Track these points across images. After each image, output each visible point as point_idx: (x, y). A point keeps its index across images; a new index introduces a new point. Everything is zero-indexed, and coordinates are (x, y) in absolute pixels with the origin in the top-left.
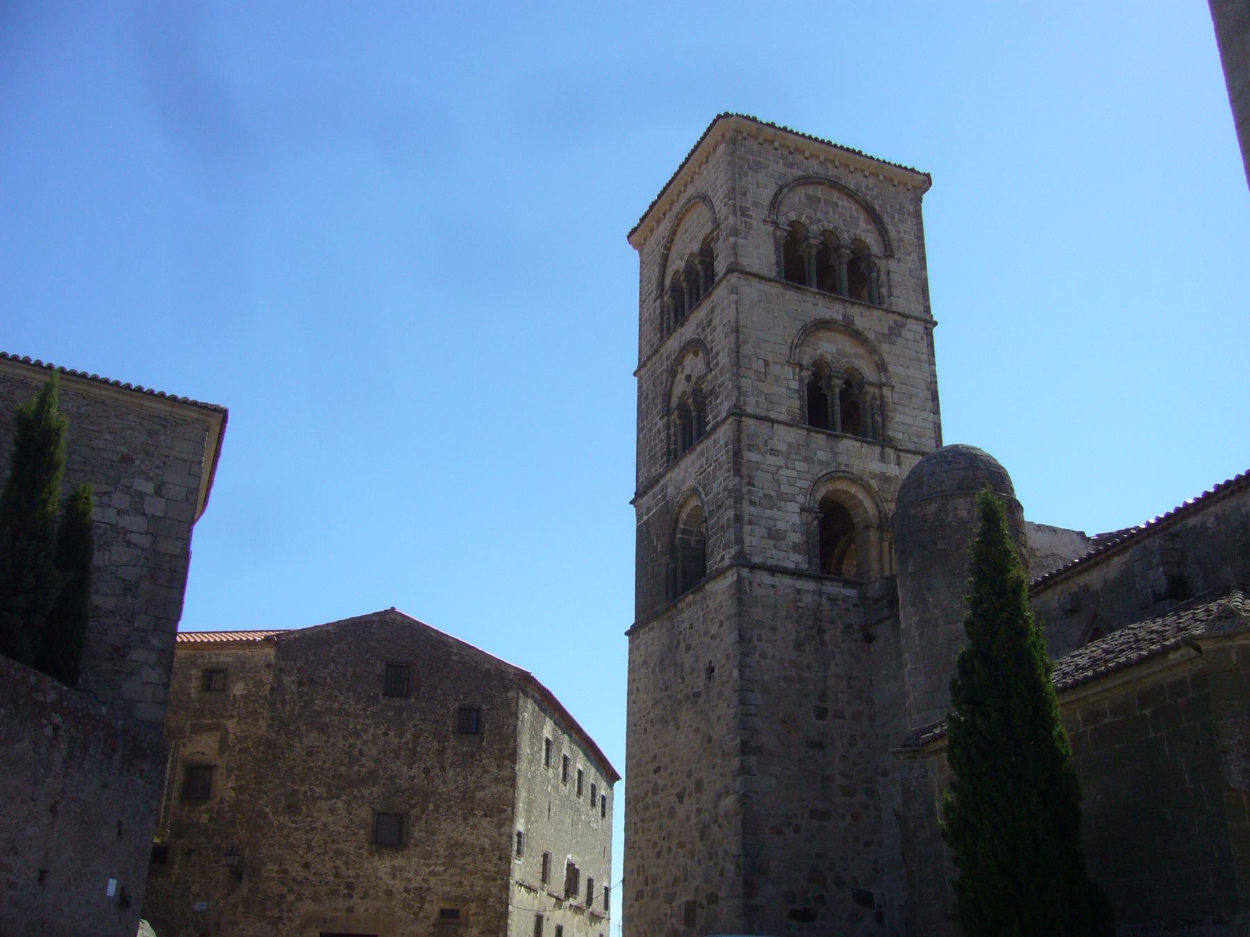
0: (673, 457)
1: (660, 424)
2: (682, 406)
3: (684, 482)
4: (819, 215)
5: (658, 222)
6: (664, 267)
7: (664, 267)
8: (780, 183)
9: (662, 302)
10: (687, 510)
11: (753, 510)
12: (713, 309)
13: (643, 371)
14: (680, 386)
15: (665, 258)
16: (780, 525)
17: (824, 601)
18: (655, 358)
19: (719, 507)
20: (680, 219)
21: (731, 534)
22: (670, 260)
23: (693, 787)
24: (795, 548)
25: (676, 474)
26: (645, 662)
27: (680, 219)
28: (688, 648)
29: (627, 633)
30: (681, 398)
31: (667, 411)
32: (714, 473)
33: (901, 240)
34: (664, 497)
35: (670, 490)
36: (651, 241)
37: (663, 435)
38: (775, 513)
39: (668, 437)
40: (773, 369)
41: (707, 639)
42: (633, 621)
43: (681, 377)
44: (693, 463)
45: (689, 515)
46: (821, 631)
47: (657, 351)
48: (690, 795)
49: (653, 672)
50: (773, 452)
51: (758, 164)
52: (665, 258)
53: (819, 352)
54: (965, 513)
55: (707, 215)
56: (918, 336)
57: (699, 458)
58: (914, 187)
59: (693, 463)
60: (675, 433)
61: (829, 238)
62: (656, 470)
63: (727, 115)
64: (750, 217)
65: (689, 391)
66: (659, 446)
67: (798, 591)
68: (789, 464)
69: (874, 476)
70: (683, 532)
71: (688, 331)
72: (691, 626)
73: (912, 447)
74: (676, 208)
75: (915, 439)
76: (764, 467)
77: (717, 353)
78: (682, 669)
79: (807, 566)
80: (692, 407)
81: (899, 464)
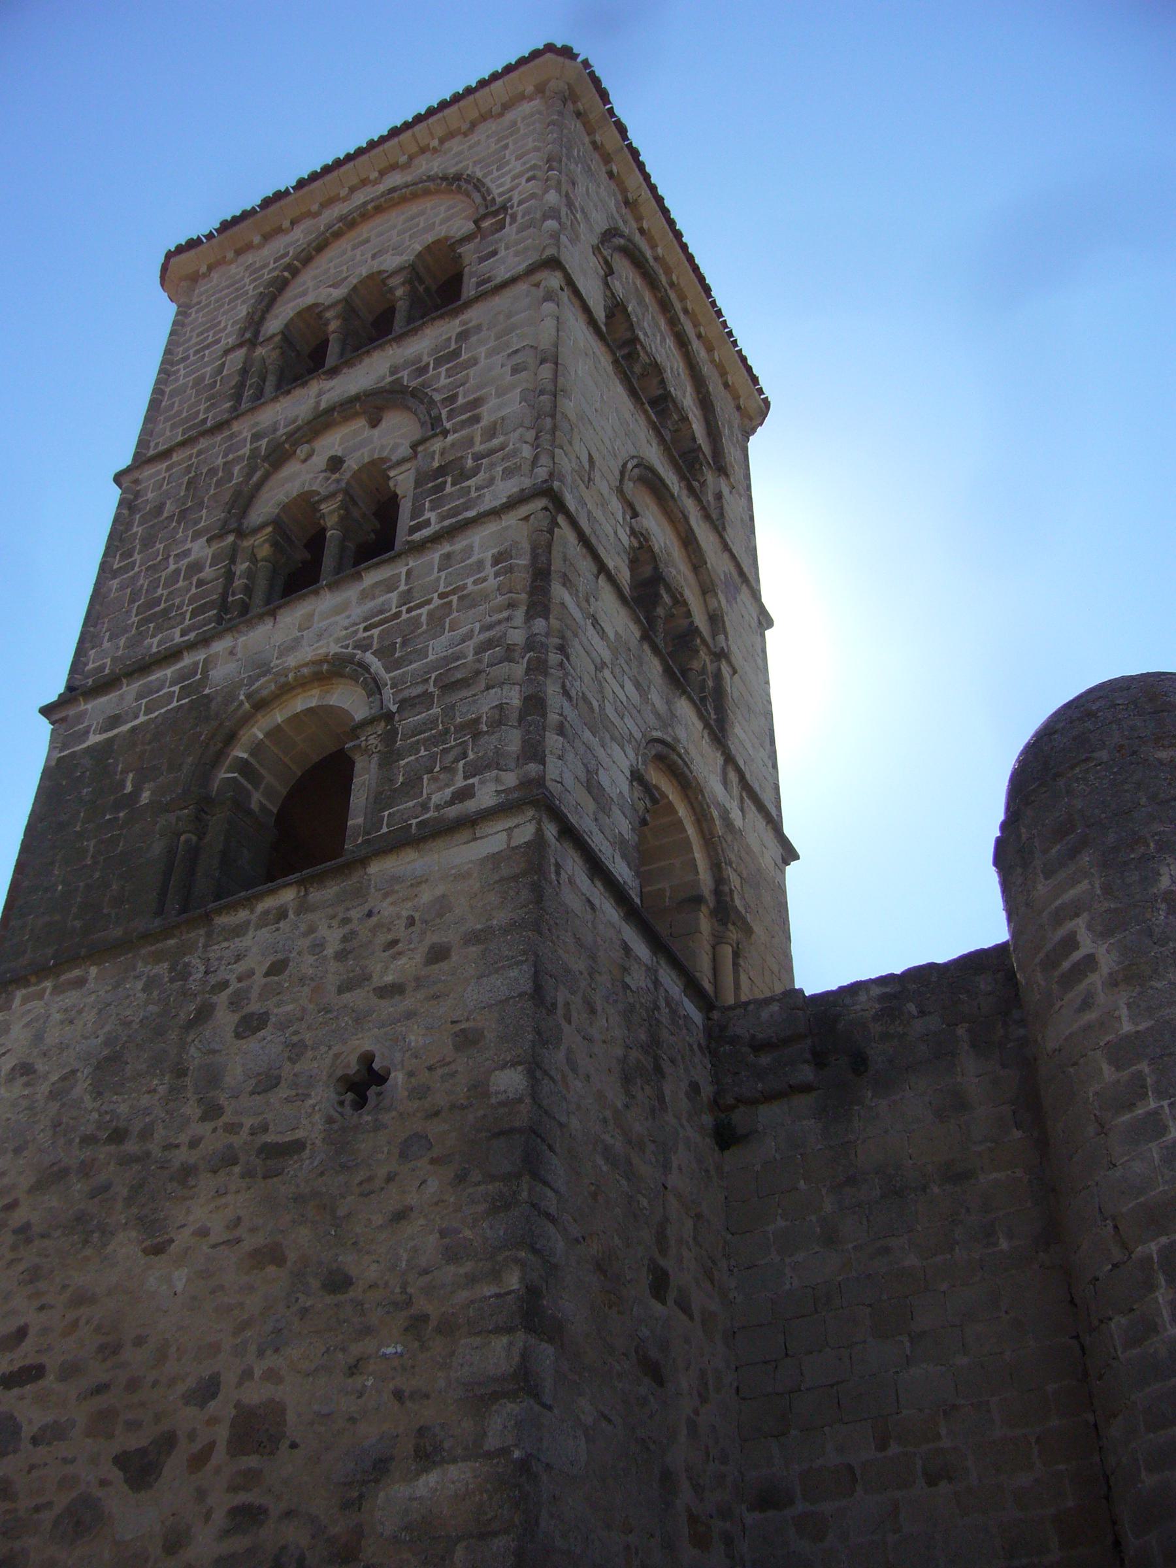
12: (463, 336)
21: (513, 740)
22: (289, 293)
23: (222, 1433)
28: (251, 1025)
39: (229, 576)
41: (358, 998)
48: (199, 1460)
60: (250, 574)
63: (567, 52)
70: (244, 767)
72: (277, 968)
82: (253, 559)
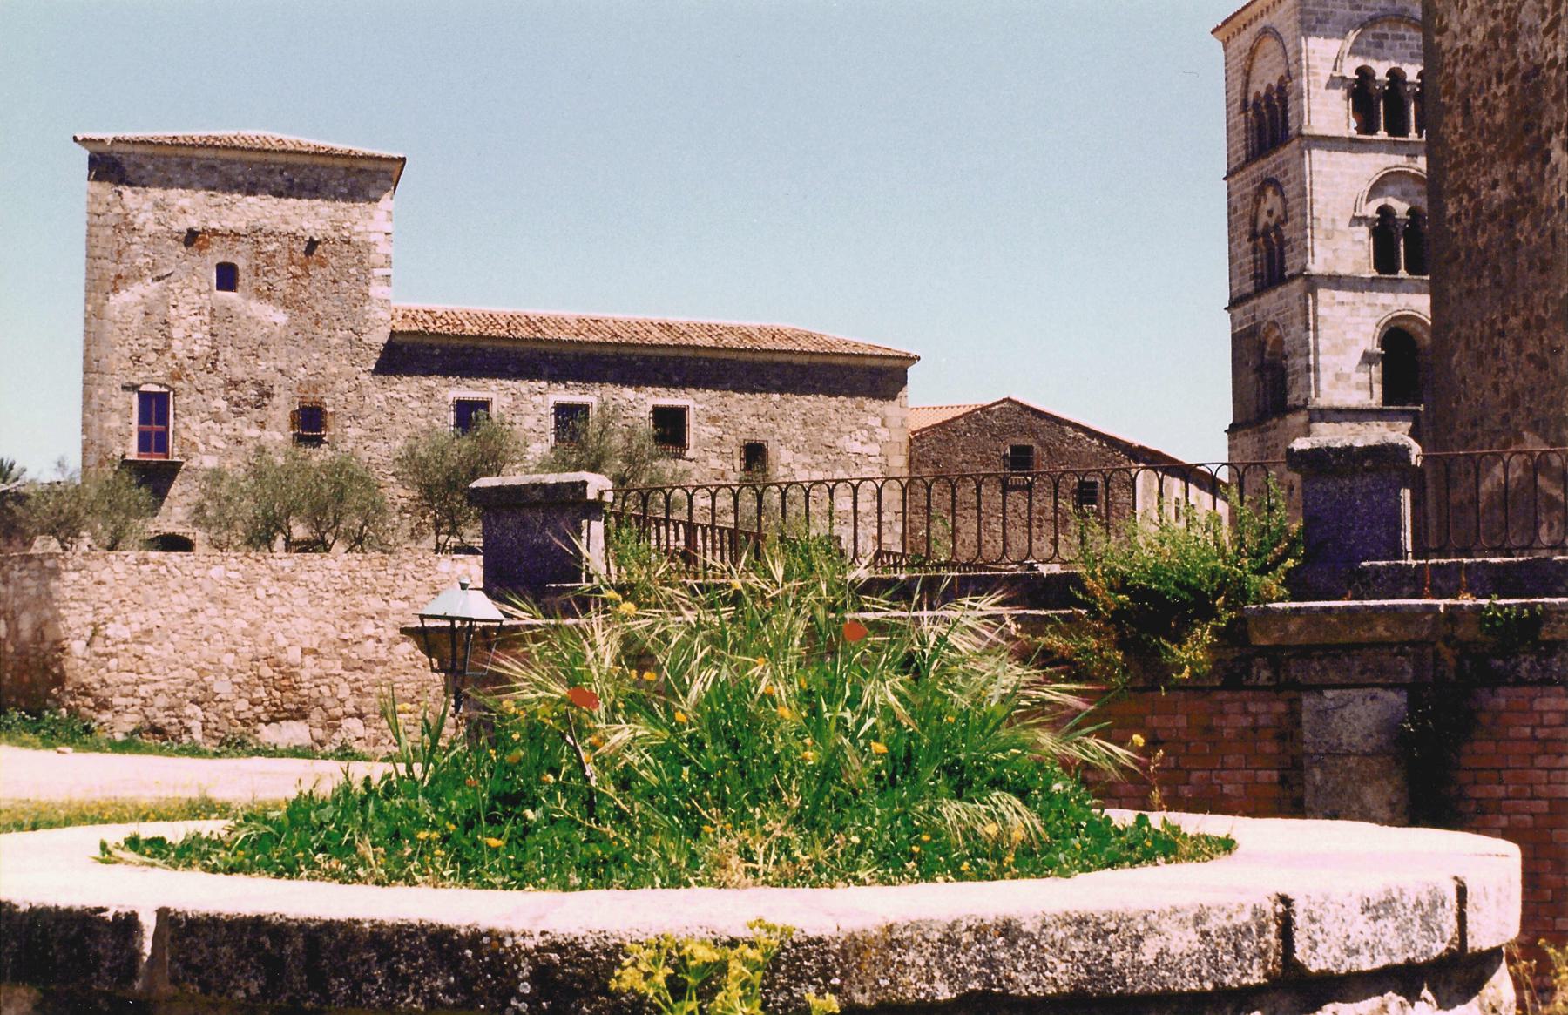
6: (1246, 84)
7: (1246, 84)
15: (1247, 74)
31: (1254, 236)
34: (1254, 318)
39: (1255, 261)
62: (1249, 287)
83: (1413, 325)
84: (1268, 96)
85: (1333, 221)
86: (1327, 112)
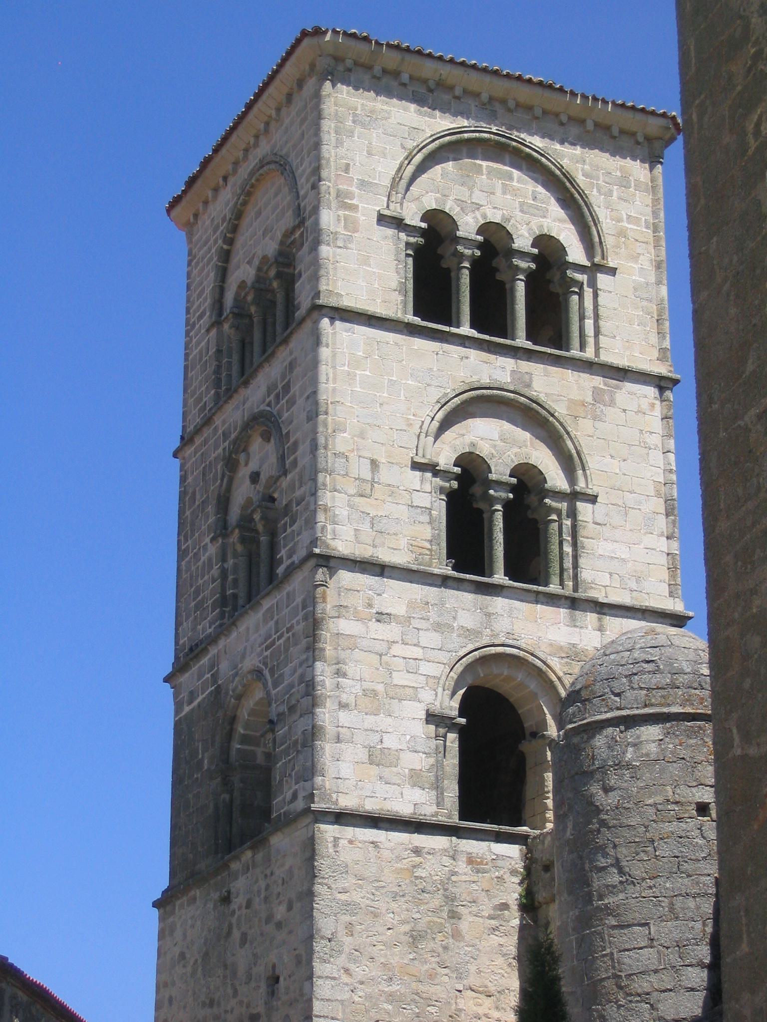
0: (232, 605)
1: (213, 550)
2: (246, 523)
3: (243, 657)
4: (478, 197)
5: (216, 190)
6: (223, 274)
7: (223, 274)
8: (411, 144)
9: (220, 334)
10: (250, 703)
11: (344, 717)
12: (291, 366)
13: (189, 451)
14: (243, 492)
15: (226, 256)
16: (390, 742)
17: (462, 866)
18: (207, 432)
19: (292, 709)
20: (248, 193)
22: (234, 260)
24: (415, 778)
25: (232, 642)
26: (182, 956)
27: (248, 193)
29: (156, 904)
30: (244, 508)
31: (222, 529)
32: (287, 650)
33: (622, 233)
34: (215, 677)
35: (224, 666)
36: (205, 221)
37: (215, 571)
38: (382, 721)
39: (224, 573)
40: (385, 475)
41: (270, 928)
42: (165, 883)
43: (244, 472)
44: (257, 629)
45: (253, 713)
46: (454, 915)
47: (208, 421)
49: (194, 973)
50: (381, 617)
51: (372, 111)
52: (226, 256)
53: (469, 438)
54: (653, 748)
55: (285, 198)
56: (644, 404)
57: (265, 621)
58: (648, 139)
59: (257, 629)
61: (494, 240)
62: (206, 628)
63: (318, 32)
64: (354, 208)
65: (256, 498)
66: (210, 591)
67: (417, 851)
68: (408, 638)
69: (557, 649)
70: (245, 739)
71: (254, 396)
72: (249, 905)
73: (625, 599)
74: (244, 171)
75: (634, 586)
76: (364, 643)
77: (296, 444)
78: (234, 974)
79: (434, 808)
80: (260, 528)
81: (601, 629)
82: (235, 556)
83: (520, 676)
84: (260, 279)
85: (374, 464)
86: (363, 267)
